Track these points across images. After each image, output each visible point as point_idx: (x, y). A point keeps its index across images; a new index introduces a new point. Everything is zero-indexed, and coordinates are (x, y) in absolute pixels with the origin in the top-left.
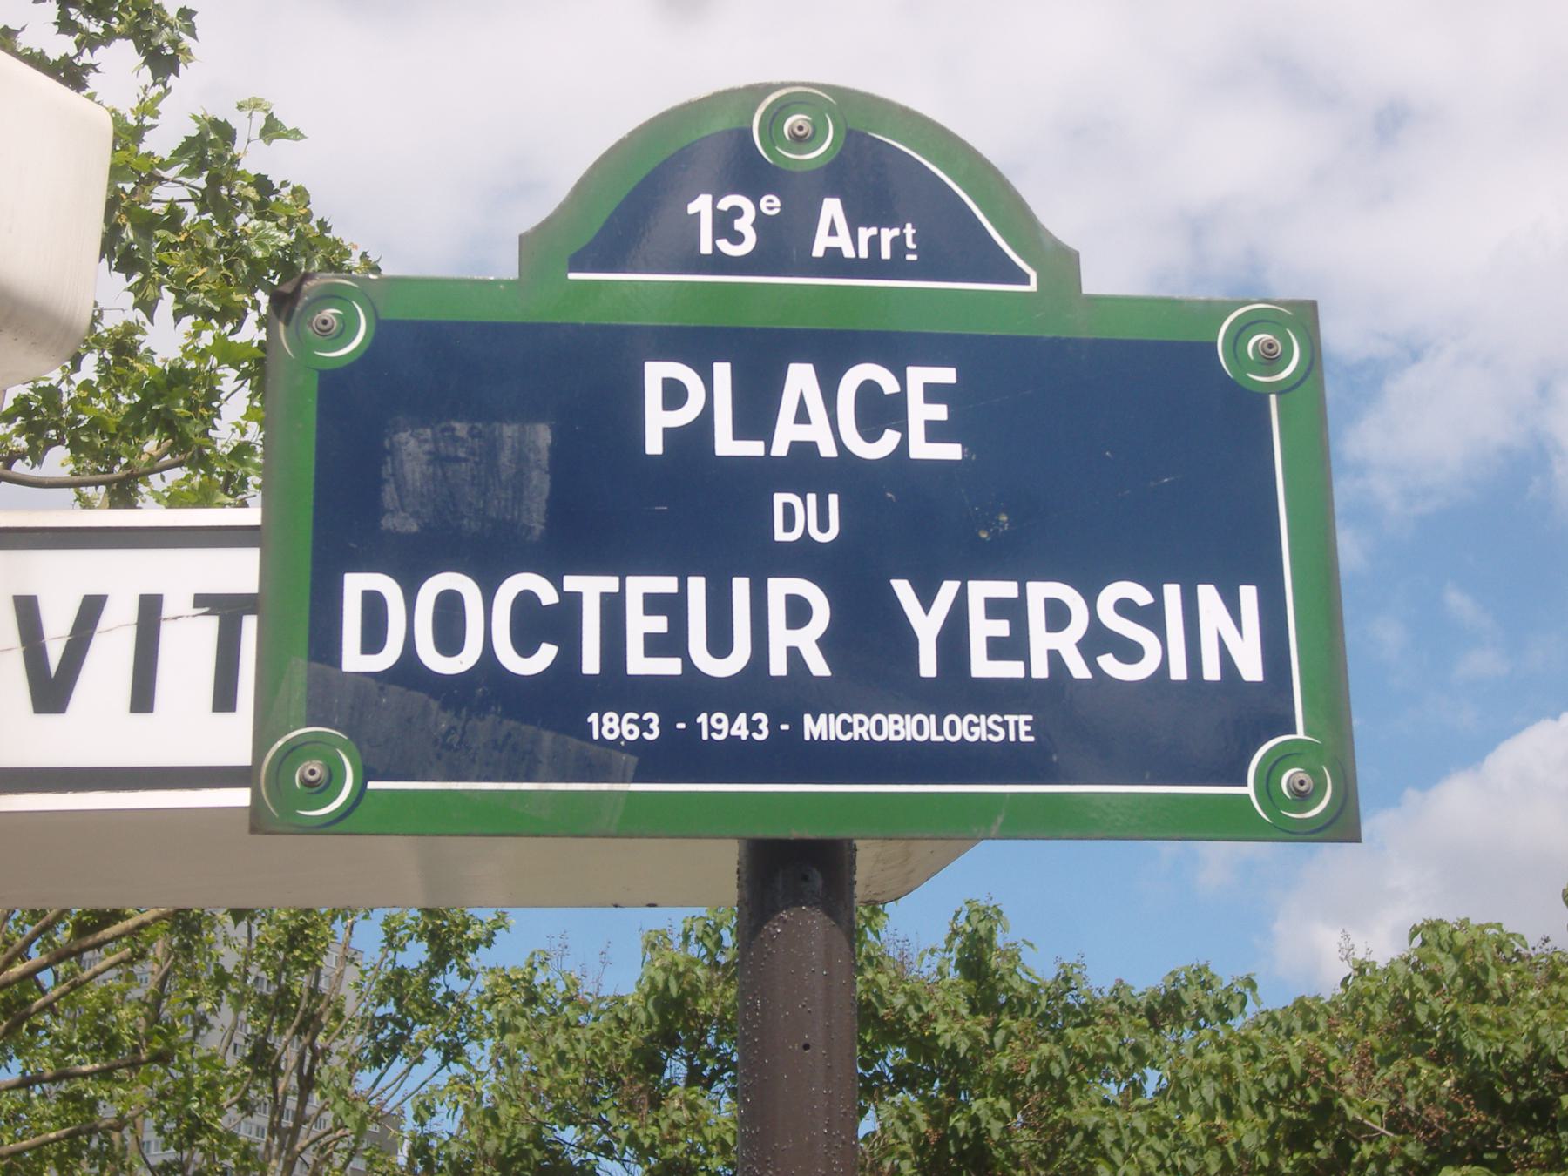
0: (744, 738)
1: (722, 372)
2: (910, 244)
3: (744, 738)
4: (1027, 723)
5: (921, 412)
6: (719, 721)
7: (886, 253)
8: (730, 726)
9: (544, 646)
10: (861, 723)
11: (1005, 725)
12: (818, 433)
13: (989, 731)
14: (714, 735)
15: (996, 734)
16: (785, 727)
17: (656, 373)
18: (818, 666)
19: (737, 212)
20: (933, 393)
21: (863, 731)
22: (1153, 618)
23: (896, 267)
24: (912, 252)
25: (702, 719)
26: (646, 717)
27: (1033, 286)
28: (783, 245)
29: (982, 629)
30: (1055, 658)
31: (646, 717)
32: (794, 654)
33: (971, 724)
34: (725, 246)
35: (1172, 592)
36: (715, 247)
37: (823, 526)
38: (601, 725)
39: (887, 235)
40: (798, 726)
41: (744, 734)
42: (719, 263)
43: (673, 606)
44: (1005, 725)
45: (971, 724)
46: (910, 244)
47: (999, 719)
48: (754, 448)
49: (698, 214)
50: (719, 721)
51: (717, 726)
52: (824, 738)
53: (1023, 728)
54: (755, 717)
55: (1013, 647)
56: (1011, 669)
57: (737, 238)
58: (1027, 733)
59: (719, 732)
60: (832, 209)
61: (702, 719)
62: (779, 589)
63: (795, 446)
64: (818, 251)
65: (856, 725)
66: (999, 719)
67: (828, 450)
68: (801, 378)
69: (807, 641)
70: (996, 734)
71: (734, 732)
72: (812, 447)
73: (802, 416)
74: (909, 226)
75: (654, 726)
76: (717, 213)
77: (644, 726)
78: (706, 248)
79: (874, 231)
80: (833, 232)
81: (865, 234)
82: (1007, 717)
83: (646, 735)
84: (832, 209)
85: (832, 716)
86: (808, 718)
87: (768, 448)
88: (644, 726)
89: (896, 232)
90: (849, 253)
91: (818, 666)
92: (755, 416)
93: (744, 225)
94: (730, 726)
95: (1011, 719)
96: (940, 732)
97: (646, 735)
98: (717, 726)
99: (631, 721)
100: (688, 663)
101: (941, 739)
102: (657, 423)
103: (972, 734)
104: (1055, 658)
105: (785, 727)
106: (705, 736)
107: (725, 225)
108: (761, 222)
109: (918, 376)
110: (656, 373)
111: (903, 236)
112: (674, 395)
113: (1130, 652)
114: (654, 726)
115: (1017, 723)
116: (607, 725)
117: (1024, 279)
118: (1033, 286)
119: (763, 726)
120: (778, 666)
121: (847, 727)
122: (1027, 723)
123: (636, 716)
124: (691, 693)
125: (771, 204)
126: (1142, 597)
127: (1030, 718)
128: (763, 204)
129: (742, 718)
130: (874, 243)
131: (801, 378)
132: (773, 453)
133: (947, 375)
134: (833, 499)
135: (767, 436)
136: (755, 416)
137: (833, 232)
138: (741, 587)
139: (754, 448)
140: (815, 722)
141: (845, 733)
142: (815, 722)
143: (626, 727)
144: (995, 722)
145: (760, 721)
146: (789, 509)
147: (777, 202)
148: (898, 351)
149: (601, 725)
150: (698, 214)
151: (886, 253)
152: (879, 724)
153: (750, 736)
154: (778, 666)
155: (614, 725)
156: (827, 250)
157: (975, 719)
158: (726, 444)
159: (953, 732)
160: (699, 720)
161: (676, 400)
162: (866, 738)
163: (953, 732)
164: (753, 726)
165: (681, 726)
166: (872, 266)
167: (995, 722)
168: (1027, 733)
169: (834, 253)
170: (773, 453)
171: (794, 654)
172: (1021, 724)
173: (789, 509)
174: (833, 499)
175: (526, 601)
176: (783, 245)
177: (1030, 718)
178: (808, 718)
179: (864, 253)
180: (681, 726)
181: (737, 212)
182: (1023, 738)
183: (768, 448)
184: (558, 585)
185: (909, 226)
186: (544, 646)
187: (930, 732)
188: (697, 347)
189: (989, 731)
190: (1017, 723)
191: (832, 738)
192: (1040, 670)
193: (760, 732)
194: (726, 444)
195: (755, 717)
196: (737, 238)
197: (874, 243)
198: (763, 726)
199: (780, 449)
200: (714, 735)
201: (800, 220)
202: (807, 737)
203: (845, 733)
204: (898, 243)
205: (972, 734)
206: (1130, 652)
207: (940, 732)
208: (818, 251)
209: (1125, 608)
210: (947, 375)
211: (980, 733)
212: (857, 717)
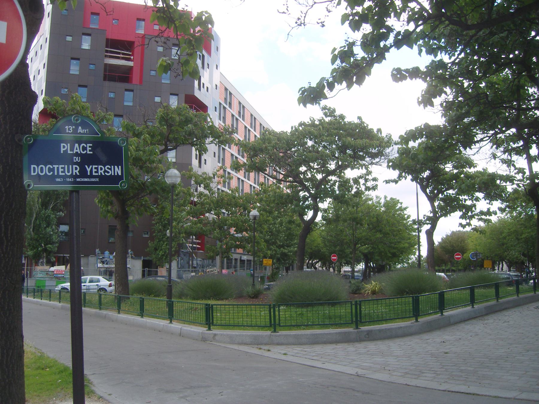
1: (69, 144)
5: (88, 149)
12: (78, 151)
17: (62, 145)
18: (78, 174)
20: (90, 147)
22: (110, 169)
23: (86, 134)
29: (94, 170)
35: (113, 167)
43: (64, 168)
55: (97, 172)
56: (97, 174)
60: (80, 128)
62: (74, 166)
67: (79, 152)
69: (77, 171)
73: (77, 149)
84: (80, 128)
91: (78, 174)
93: (71, 129)
102: (62, 150)
107: (69, 129)
108: (73, 129)
109: (88, 145)
110: (62, 145)
112: (64, 147)
113: (108, 172)
120: (74, 174)
124: (66, 176)
126: (110, 167)
131: (77, 145)
133: (91, 145)
154: (74, 174)
158: (69, 152)
166: (84, 134)
175: (49, 168)
194: (69, 152)
201: (77, 129)
206: (108, 172)
209: (108, 168)
210: (91, 145)
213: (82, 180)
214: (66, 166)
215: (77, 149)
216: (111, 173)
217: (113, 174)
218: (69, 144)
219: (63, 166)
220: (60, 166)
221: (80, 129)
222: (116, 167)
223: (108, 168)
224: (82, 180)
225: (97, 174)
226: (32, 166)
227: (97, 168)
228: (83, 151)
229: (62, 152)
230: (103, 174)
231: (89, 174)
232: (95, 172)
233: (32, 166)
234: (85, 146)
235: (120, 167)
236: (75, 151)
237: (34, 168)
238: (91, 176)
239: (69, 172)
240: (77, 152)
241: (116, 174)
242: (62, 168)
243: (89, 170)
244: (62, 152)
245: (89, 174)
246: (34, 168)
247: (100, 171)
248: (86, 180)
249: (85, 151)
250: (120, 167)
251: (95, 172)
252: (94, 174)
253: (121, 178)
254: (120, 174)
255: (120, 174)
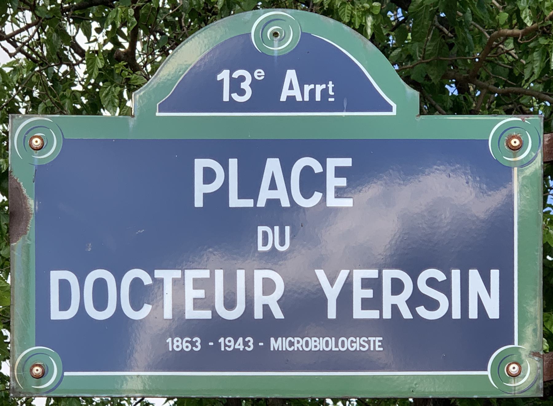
0: (241, 350)
1: (233, 163)
2: (331, 93)
3: (241, 350)
4: (379, 341)
5: (333, 182)
6: (230, 341)
7: (318, 98)
8: (235, 345)
9: (146, 306)
10: (298, 342)
11: (368, 342)
12: (281, 194)
13: (361, 345)
14: (227, 348)
15: (364, 347)
16: (261, 344)
17: (200, 164)
18: (278, 314)
19: (242, 79)
20: (340, 172)
21: (299, 345)
22: (445, 287)
23: (324, 106)
24: (331, 96)
25: (221, 340)
26: (194, 340)
27: (394, 113)
28: (266, 95)
29: (360, 294)
30: (395, 308)
31: (194, 340)
32: (266, 308)
33: (352, 342)
34: (235, 96)
35: (456, 274)
36: (230, 97)
37: (282, 243)
38: (173, 344)
39: (319, 88)
40: (268, 344)
41: (241, 348)
42: (233, 106)
43: (206, 284)
44: (368, 342)
45: (352, 342)
46: (331, 93)
47: (366, 339)
48: (248, 203)
49: (223, 80)
50: (230, 341)
51: (228, 344)
52: (280, 349)
53: (378, 344)
54: (247, 340)
55: (375, 303)
56: (374, 314)
57: (242, 93)
58: (379, 346)
59: (229, 347)
60: (291, 75)
61: (221, 340)
62: (259, 275)
63: (270, 202)
64: (283, 98)
65: (296, 342)
66: (366, 339)
67: (285, 203)
68: (273, 166)
69: (272, 301)
70: (364, 347)
71: (237, 347)
72: (277, 202)
73: (273, 186)
74: (331, 83)
75: (198, 344)
76: (231, 79)
77: (193, 344)
78: (226, 98)
79: (312, 86)
80: (291, 87)
81: (307, 88)
82: (369, 338)
83: (194, 348)
84: (291, 75)
85: (284, 339)
86: (272, 339)
87: (255, 203)
88: (193, 344)
89: (324, 86)
90: (299, 98)
91: (278, 314)
92: (249, 186)
93: (245, 86)
94: (235, 345)
95: (372, 339)
96: (337, 346)
97: (194, 348)
98: (228, 344)
99: (187, 342)
100: (214, 313)
101: (337, 349)
102: (201, 190)
103: (352, 347)
104: (395, 308)
105: (261, 344)
106: (223, 349)
107: (236, 86)
108: (254, 84)
109: (332, 163)
110: (200, 164)
111: (327, 88)
112: (209, 175)
113: (433, 305)
114: (198, 344)
115: (374, 341)
116: (176, 344)
117: (390, 109)
118: (394, 113)
119: (251, 344)
120: (258, 314)
121: (291, 344)
122: (379, 341)
123: (190, 339)
124: (215, 328)
125: (260, 74)
126: (440, 276)
127: (381, 339)
128: (256, 74)
129: (240, 340)
130: (312, 93)
131: (273, 166)
132: (258, 205)
133: (347, 162)
134: (287, 229)
135: (255, 196)
136: (249, 186)
137: (291, 87)
138: (241, 275)
139: (248, 203)
140: (276, 342)
141: (290, 347)
142: (276, 342)
143: (185, 344)
144: (364, 341)
145: (249, 341)
146: (265, 234)
147: (263, 73)
148: (322, 150)
149: (173, 344)
150: (223, 80)
151: (318, 98)
152: (307, 342)
153: (244, 349)
154: (258, 314)
155: (179, 344)
156: (288, 97)
157: (354, 340)
158: (234, 201)
159: (343, 346)
160: (220, 341)
161: (210, 179)
162: (301, 349)
163: (343, 346)
164: (246, 344)
165: (211, 344)
166: (311, 105)
167: (364, 341)
168: (379, 346)
169: (291, 99)
170: (258, 205)
171: (266, 308)
172: (377, 342)
173: (265, 234)
174: (287, 229)
175: (136, 282)
176: (266, 95)
177: (381, 339)
178: (272, 339)
179: (307, 98)
180: (211, 344)
181: (242, 79)
182: (378, 349)
183: (255, 203)
184: (152, 274)
185: (331, 83)
186: (146, 306)
187: (332, 346)
188: (220, 151)
189: (361, 345)
190: (374, 341)
191: (284, 349)
192: (387, 314)
193: (249, 347)
194: (234, 201)
195: (247, 340)
196: (242, 93)
197: (312, 93)
198: (251, 344)
199: (261, 203)
200: (227, 348)
201: (275, 82)
202: (272, 349)
203: (290, 347)
204: (324, 92)
205: (352, 347)
206: (433, 305)
207: (337, 346)
208: (283, 98)
209: (431, 282)
210: (347, 162)
211: (356, 346)
212: (296, 339)
213: (299, 343)
214: (219, 274)
215: (273, 186)
216: (448, 306)
217: (456, 314)
218: (233, 163)
219: (205, 274)
220: (191, 275)
221: (291, 86)
222: (474, 275)
223: (431, 282)
224: (299, 343)
225: (374, 314)
226: (56, 276)
227: (375, 284)
228: (306, 193)
229: (199, 202)
230: (407, 314)
231: (332, 314)
232: (366, 304)
233: (56, 276)
234: (317, 168)
235: (495, 274)
236: (265, 194)
237: (64, 285)
238: (346, 324)
239: (230, 304)
240: (273, 203)
241: (473, 314)
242: (198, 284)
243: (332, 293)
244: (199, 202)
245: (332, 314)
246: (64, 285)
247: (388, 299)
248: (317, 344)
249: (317, 196)
250: (495, 274)
251: (366, 304)
252: (359, 313)
253: (498, 331)
254: (493, 313)
255: (493, 313)
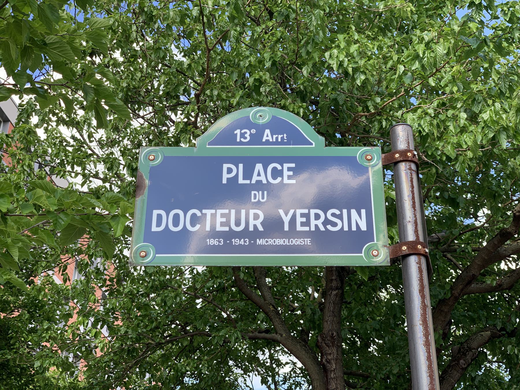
1: (241, 166)
2: (285, 138)
5: (286, 173)
7: (279, 140)
13: (300, 242)
17: (225, 166)
18: (261, 228)
19: (246, 133)
20: (289, 169)
23: (282, 143)
25: (233, 240)
27: (314, 146)
28: (256, 139)
29: (299, 220)
30: (316, 226)
34: (242, 140)
35: (345, 211)
37: (263, 198)
39: (280, 136)
41: (243, 243)
43: (227, 216)
44: (304, 241)
46: (285, 138)
48: (248, 182)
51: (236, 242)
53: (309, 242)
55: (307, 223)
56: (307, 229)
60: (267, 131)
61: (233, 240)
62: (252, 212)
63: (257, 181)
64: (264, 140)
67: (264, 182)
68: (259, 167)
73: (259, 175)
75: (222, 242)
77: (220, 242)
78: (238, 140)
81: (275, 136)
84: (267, 131)
86: (258, 240)
87: (251, 182)
88: (220, 242)
89: (282, 136)
90: (271, 140)
91: (261, 228)
92: (248, 175)
96: (289, 242)
98: (236, 242)
100: (230, 228)
102: (225, 176)
104: (316, 226)
107: (243, 135)
108: (251, 135)
109: (286, 166)
110: (225, 166)
111: (284, 136)
112: (230, 171)
113: (335, 224)
114: (222, 242)
116: (211, 242)
118: (314, 146)
119: (247, 242)
120: (251, 229)
121: (267, 242)
124: (231, 235)
125: (253, 131)
126: (337, 212)
128: (252, 131)
129: (242, 240)
130: (277, 138)
131: (259, 167)
133: (293, 165)
134: (265, 192)
136: (248, 175)
137: (267, 136)
138: (243, 212)
139: (248, 182)
143: (215, 242)
146: (255, 195)
148: (281, 160)
151: (279, 140)
152: (274, 241)
154: (251, 229)
159: (292, 242)
164: (245, 242)
166: (277, 143)
169: (267, 141)
171: (255, 226)
173: (255, 195)
174: (265, 192)
176: (256, 139)
178: (258, 240)
179: (274, 140)
181: (246, 133)
183: (251, 182)
184: (201, 211)
187: (287, 242)
188: (236, 161)
189: (300, 242)
192: (313, 228)
194: (241, 181)
196: (246, 138)
197: (277, 138)
198: (247, 242)
199: (253, 182)
204: (282, 138)
206: (335, 224)
207: (289, 242)
208: (264, 140)
209: (333, 215)
210: (293, 165)
211: (298, 243)
